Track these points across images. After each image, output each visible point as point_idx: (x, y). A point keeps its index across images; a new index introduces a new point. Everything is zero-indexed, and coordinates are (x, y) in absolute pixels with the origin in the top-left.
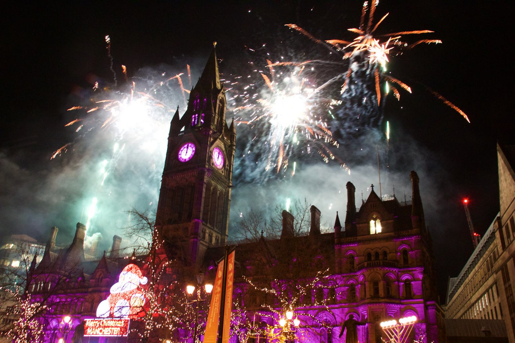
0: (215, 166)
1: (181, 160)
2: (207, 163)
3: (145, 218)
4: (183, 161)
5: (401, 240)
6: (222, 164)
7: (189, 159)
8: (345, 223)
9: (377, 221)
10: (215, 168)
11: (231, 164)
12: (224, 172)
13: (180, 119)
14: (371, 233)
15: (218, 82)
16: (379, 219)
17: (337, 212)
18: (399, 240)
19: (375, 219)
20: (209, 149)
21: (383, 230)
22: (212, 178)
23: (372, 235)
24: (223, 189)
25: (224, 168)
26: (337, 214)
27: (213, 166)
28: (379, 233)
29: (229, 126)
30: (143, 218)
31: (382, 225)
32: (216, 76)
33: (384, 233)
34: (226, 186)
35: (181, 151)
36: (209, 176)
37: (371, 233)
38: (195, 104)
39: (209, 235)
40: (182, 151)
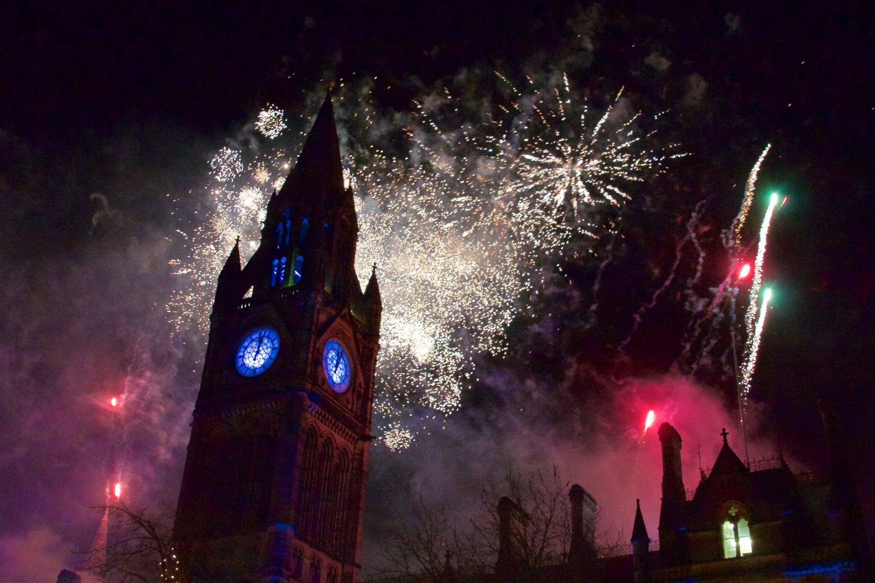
1: (244, 371)
3: (147, 524)
4: (247, 373)
5: (804, 572)
6: (348, 380)
7: (263, 369)
8: (660, 529)
9: (739, 525)
12: (351, 401)
14: (727, 557)
16: (746, 519)
17: (638, 501)
18: (799, 573)
19: (734, 520)
20: (315, 343)
21: (755, 547)
23: (730, 559)
24: (350, 445)
25: (350, 392)
26: (638, 505)
27: (325, 387)
28: (746, 556)
29: (363, 285)
30: (142, 525)
31: (754, 534)
33: (760, 555)
34: (356, 437)
35: (242, 349)
36: (314, 412)
37: (727, 557)
39: (312, 564)
40: (246, 348)
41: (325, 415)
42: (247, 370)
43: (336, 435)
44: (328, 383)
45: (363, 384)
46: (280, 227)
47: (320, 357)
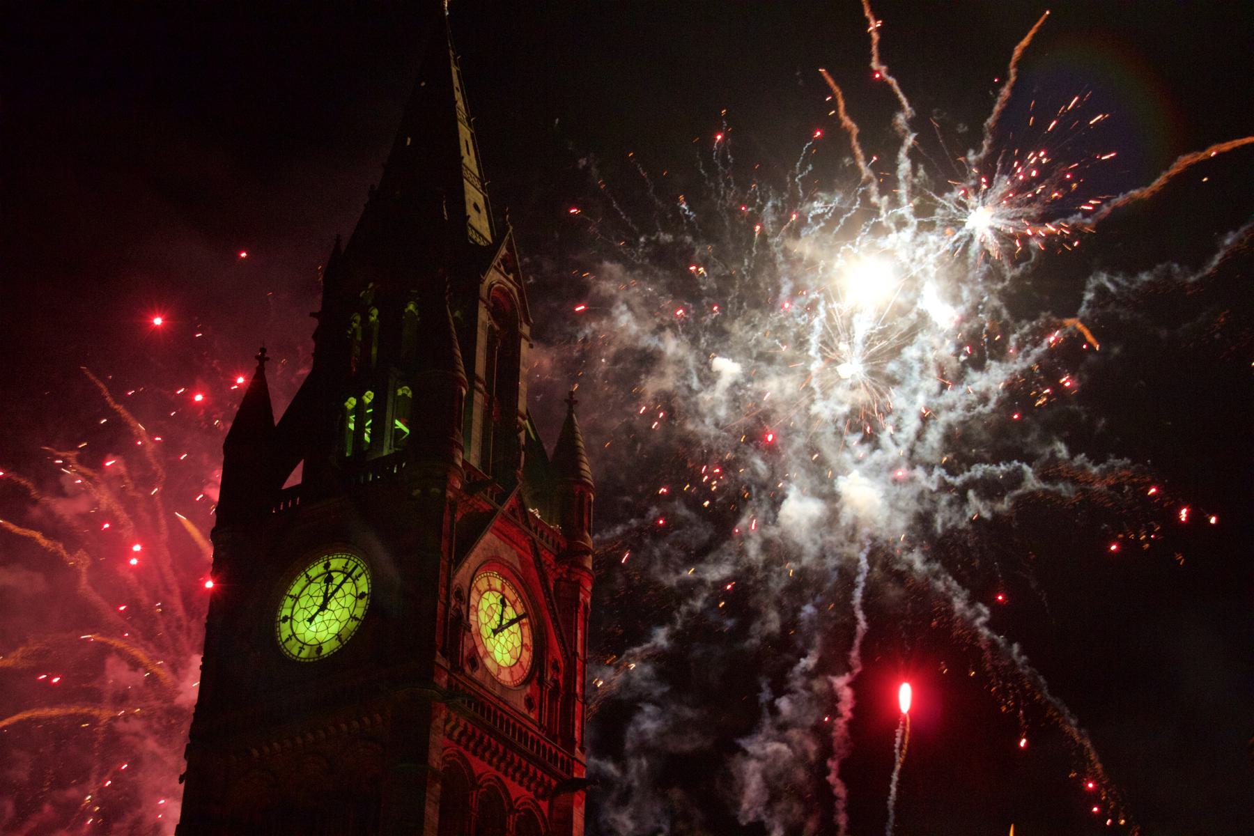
0: (487, 670)
1: (295, 651)
2: (440, 659)
4: (304, 654)
6: (527, 656)
7: (335, 644)
10: (488, 685)
11: (575, 654)
12: (536, 701)
13: (276, 422)
15: (476, 207)
20: (449, 580)
22: (471, 745)
25: (535, 682)
27: (478, 675)
32: (466, 173)
34: (554, 783)
35: (289, 602)
36: (456, 733)
38: (359, 338)
40: (296, 598)
41: (481, 738)
42: (301, 649)
43: (507, 781)
44: (484, 665)
45: (562, 665)
46: (355, 325)
47: (464, 607)
